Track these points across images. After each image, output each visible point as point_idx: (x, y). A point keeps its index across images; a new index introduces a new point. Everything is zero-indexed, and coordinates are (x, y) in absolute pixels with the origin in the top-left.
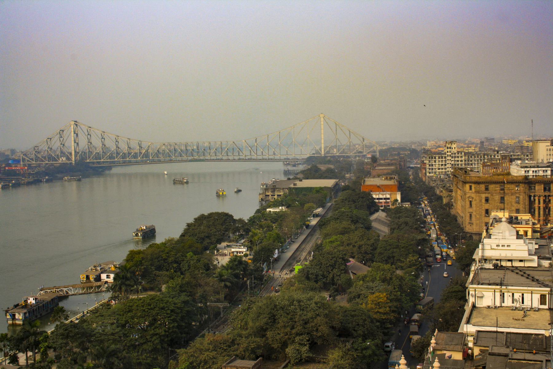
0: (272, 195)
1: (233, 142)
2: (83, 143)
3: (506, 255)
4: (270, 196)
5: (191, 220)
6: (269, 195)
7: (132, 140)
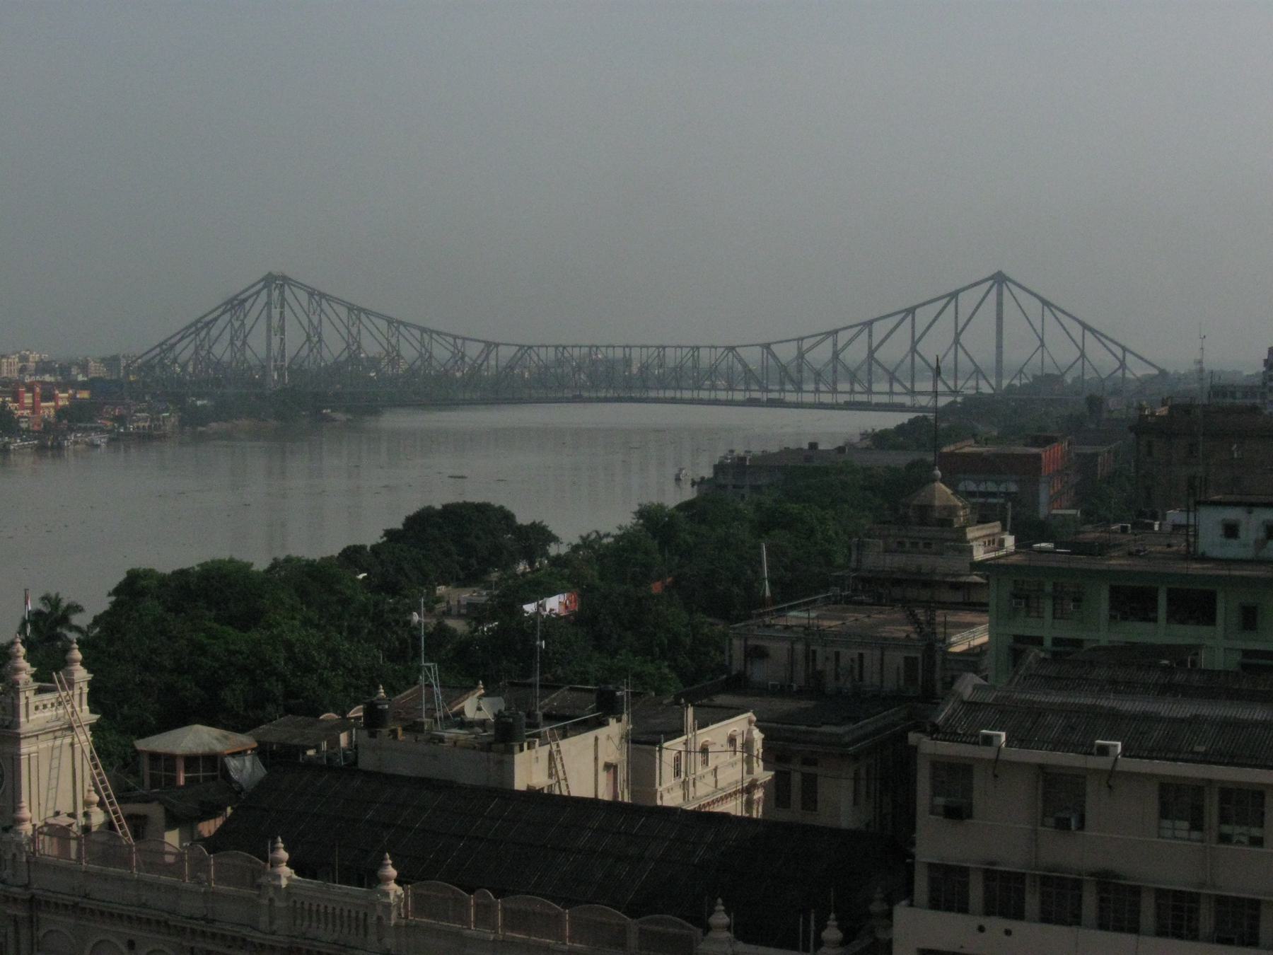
0: (734, 487)
1: (732, 349)
2: (334, 347)
3: (640, 505)
4: (730, 487)
5: (397, 524)
6: (724, 487)
7: (438, 333)
